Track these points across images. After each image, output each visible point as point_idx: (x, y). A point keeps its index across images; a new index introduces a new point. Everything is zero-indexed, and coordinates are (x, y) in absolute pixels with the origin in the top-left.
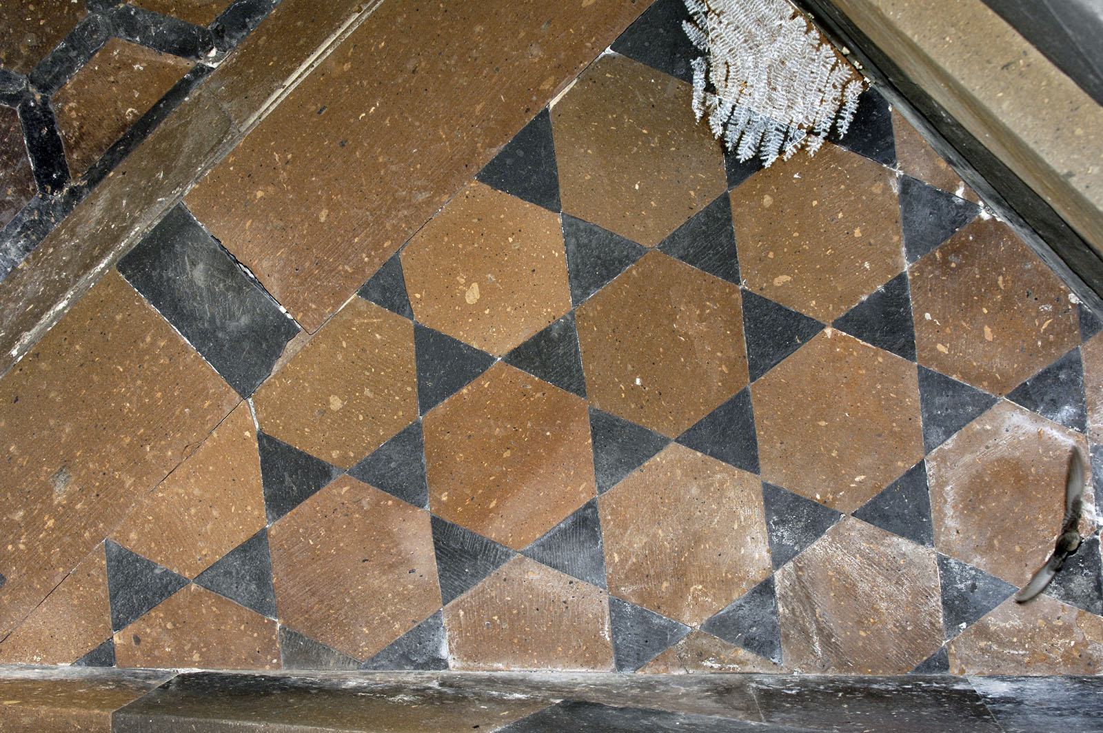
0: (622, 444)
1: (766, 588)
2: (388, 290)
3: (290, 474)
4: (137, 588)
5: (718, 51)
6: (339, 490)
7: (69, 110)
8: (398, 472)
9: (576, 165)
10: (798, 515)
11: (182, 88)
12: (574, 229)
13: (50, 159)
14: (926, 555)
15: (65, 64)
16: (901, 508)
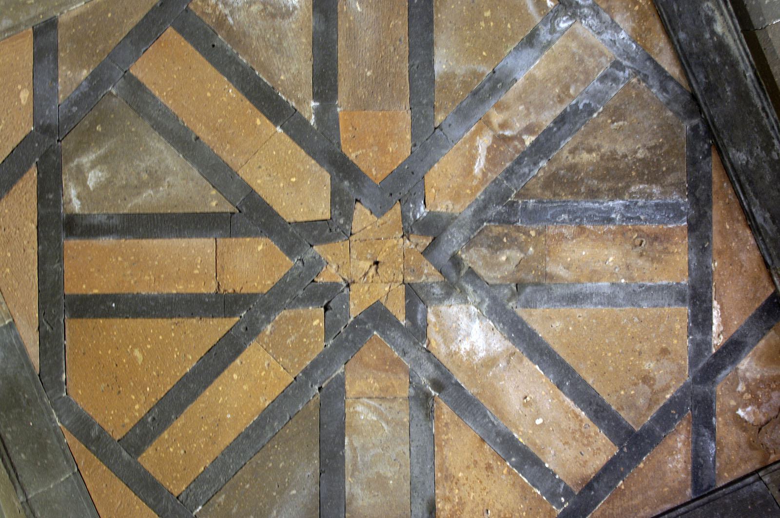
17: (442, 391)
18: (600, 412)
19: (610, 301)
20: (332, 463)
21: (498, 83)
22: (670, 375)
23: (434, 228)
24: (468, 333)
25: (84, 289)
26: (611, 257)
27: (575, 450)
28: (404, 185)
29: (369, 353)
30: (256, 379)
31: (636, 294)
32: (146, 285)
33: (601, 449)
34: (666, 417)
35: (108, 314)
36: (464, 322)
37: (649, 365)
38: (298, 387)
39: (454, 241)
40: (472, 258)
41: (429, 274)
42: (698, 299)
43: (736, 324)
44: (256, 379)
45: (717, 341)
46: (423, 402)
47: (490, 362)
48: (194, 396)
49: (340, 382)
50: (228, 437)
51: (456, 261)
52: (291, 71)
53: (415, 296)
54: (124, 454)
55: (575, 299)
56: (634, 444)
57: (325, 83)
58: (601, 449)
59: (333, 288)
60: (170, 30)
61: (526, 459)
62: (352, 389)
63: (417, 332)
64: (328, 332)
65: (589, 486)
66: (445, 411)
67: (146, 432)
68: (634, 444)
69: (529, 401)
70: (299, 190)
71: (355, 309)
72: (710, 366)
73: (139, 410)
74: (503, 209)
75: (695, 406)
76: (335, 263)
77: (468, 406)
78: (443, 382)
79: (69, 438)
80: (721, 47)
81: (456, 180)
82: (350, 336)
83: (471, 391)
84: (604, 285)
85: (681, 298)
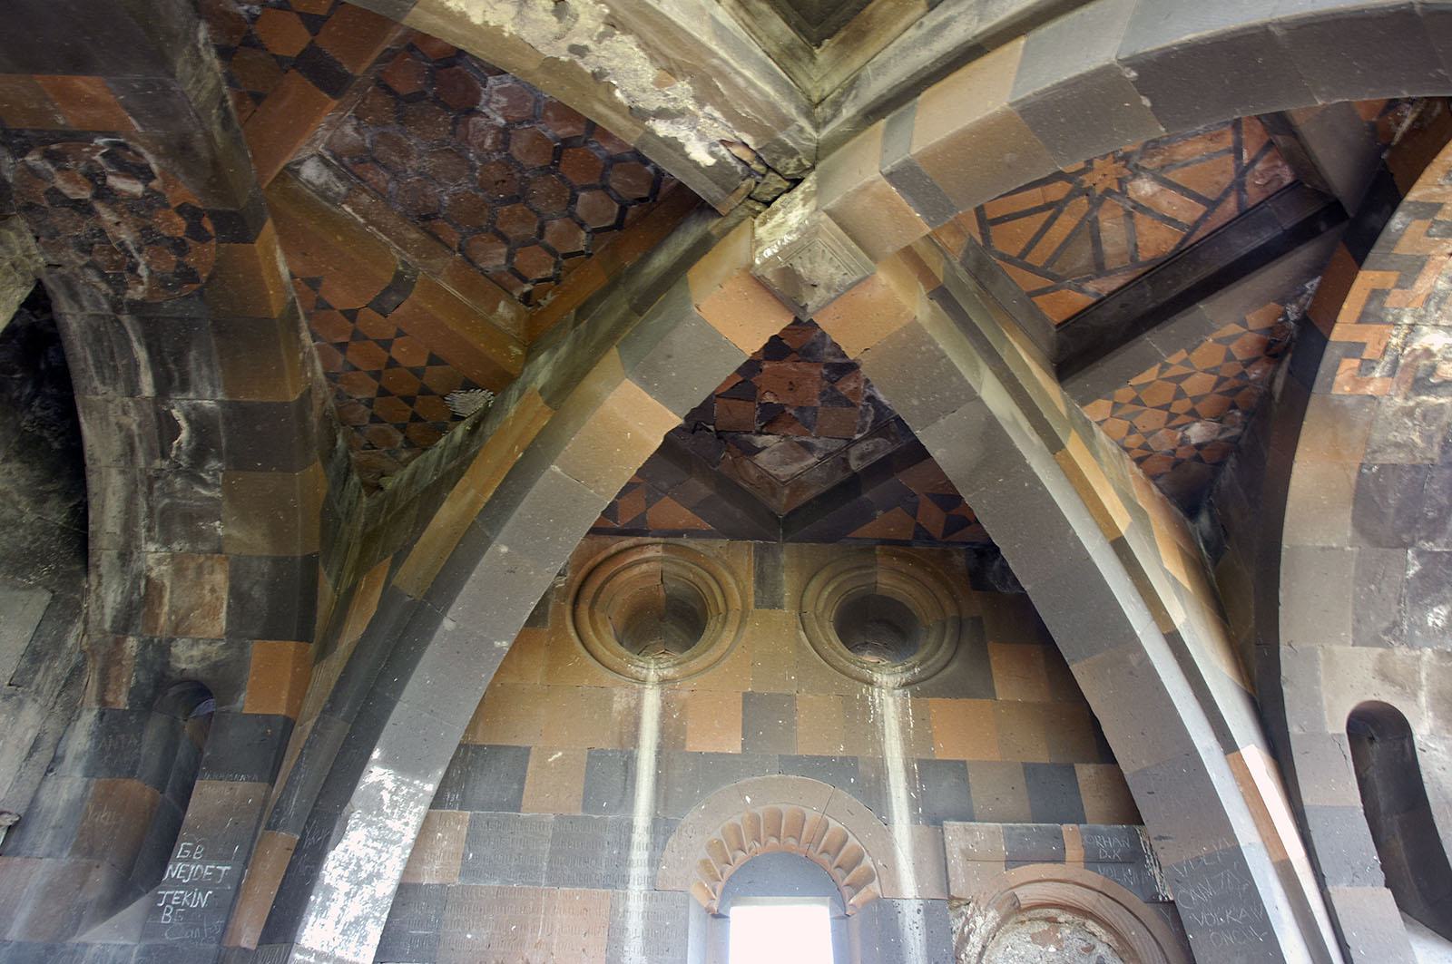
0: (377, 375)
1: (351, 398)
2: (400, 334)
3: (351, 315)
4: (313, 283)
5: (468, 395)
6: (350, 325)
7: (439, 223)
8: (356, 335)
9: (437, 369)
10: (370, 403)
11: (449, 248)
12: (424, 369)
13: (426, 218)
14: (366, 423)
15: (451, 223)
16: (374, 419)
18: (1199, 198)
19: (1200, 161)
20: (1096, 242)
22: (1226, 180)
24: (1145, 188)
25: (994, 216)
26: (1200, 146)
29: (1106, 205)
30: (1065, 224)
32: (1017, 209)
33: (1201, 209)
34: (1226, 193)
35: (1005, 221)
36: (1142, 185)
38: (1081, 223)
39: (1135, 159)
40: (1142, 163)
43: (1253, 154)
44: (1065, 224)
46: (1129, 215)
47: (1154, 195)
48: (1042, 236)
49: (1096, 218)
50: (1057, 245)
51: (1136, 166)
53: (1121, 182)
54: (1020, 261)
55: (1186, 165)
56: (1212, 205)
58: (1201, 209)
59: (1090, 188)
61: (1171, 221)
62: (1100, 219)
63: (1124, 193)
64: (1089, 203)
66: (1138, 215)
67: (1026, 251)
69: (1173, 204)
72: (1242, 172)
73: (1022, 246)
75: (1239, 186)
77: (1145, 210)
79: (998, 262)
82: (1097, 203)
84: (1198, 157)
85: (1229, 151)
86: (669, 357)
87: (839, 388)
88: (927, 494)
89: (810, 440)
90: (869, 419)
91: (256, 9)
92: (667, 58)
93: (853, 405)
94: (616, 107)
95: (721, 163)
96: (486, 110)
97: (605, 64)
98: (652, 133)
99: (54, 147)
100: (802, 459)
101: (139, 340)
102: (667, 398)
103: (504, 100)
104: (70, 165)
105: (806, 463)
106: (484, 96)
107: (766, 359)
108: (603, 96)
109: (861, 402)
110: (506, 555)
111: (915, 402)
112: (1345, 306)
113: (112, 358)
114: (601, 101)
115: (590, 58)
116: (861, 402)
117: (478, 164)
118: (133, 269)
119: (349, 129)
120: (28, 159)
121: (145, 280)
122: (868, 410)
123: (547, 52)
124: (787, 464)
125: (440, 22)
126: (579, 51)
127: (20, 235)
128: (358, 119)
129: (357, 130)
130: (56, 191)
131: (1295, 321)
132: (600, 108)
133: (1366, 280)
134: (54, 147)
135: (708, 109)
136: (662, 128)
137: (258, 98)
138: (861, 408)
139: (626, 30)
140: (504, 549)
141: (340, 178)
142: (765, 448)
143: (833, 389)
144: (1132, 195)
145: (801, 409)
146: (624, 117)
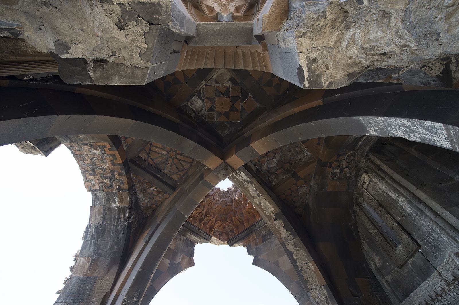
17: (163, 149)
18: (153, 151)
21: (171, 166)
23: (170, 157)
27: (153, 149)
28: (173, 159)
31: (156, 158)
34: (149, 153)
37: (152, 155)
41: (168, 155)
42: (152, 160)
43: (149, 159)
45: (149, 157)
52: (183, 163)
53: (169, 153)
56: (150, 150)
57: (180, 162)
58: (152, 149)
60: (191, 162)
61: (156, 147)
64: (172, 150)
65: (151, 147)
66: (163, 148)
68: (150, 150)
70: (178, 156)
71: (172, 151)
72: (149, 156)
74: (167, 160)
76: (174, 154)
77: (162, 149)
78: (164, 149)
80: (159, 175)
81: (170, 160)
83: (162, 150)
86: (251, 157)
87: (211, 104)
88: (183, 84)
89: (216, 85)
90: (202, 93)
91: (302, 186)
92: (247, 190)
93: (207, 98)
94: (255, 185)
95: (239, 172)
96: (276, 161)
97: (255, 192)
98: (250, 179)
99: (343, 177)
100: (218, 76)
101: (358, 145)
102: (253, 150)
103: (273, 163)
104: (344, 174)
105: (216, 75)
106: (276, 164)
107: (229, 112)
108: (256, 186)
109: (205, 99)
110: (300, 137)
111: (199, 150)
112: (120, 157)
113: (367, 142)
114: (257, 186)
115: (257, 194)
116: (205, 99)
117: (280, 153)
118: (348, 156)
119: (299, 157)
120: (349, 175)
121: (348, 154)
122: (203, 96)
123: (263, 197)
124: (222, 74)
125: (276, 208)
126: (259, 196)
127: (361, 165)
128: (297, 159)
129: (298, 157)
130: (349, 170)
131: (122, 141)
132: (257, 185)
133: (120, 161)
134: (343, 177)
135: (241, 181)
136: (248, 179)
137: (310, 175)
138: (205, 97)
139: (252, 196)
140: (300, 138)
141: (305, 151)
142: (228, 81)
143: (212, 103)
144: (166, 151)
145: (219, 96)
146: (254, 182)
